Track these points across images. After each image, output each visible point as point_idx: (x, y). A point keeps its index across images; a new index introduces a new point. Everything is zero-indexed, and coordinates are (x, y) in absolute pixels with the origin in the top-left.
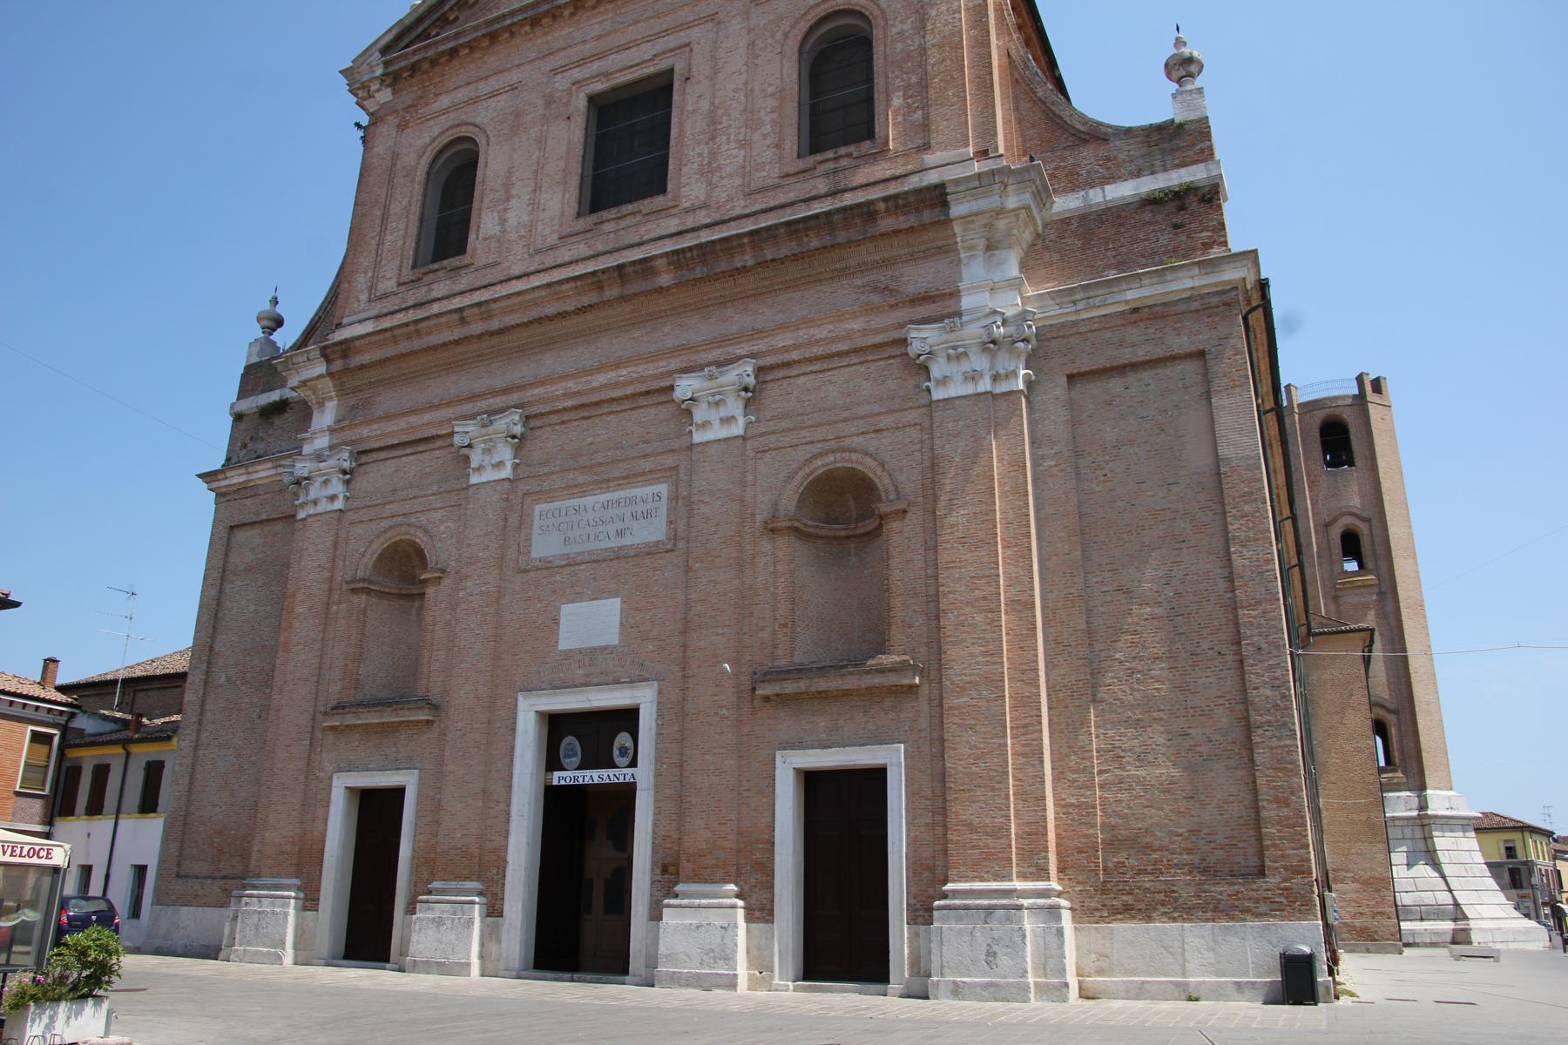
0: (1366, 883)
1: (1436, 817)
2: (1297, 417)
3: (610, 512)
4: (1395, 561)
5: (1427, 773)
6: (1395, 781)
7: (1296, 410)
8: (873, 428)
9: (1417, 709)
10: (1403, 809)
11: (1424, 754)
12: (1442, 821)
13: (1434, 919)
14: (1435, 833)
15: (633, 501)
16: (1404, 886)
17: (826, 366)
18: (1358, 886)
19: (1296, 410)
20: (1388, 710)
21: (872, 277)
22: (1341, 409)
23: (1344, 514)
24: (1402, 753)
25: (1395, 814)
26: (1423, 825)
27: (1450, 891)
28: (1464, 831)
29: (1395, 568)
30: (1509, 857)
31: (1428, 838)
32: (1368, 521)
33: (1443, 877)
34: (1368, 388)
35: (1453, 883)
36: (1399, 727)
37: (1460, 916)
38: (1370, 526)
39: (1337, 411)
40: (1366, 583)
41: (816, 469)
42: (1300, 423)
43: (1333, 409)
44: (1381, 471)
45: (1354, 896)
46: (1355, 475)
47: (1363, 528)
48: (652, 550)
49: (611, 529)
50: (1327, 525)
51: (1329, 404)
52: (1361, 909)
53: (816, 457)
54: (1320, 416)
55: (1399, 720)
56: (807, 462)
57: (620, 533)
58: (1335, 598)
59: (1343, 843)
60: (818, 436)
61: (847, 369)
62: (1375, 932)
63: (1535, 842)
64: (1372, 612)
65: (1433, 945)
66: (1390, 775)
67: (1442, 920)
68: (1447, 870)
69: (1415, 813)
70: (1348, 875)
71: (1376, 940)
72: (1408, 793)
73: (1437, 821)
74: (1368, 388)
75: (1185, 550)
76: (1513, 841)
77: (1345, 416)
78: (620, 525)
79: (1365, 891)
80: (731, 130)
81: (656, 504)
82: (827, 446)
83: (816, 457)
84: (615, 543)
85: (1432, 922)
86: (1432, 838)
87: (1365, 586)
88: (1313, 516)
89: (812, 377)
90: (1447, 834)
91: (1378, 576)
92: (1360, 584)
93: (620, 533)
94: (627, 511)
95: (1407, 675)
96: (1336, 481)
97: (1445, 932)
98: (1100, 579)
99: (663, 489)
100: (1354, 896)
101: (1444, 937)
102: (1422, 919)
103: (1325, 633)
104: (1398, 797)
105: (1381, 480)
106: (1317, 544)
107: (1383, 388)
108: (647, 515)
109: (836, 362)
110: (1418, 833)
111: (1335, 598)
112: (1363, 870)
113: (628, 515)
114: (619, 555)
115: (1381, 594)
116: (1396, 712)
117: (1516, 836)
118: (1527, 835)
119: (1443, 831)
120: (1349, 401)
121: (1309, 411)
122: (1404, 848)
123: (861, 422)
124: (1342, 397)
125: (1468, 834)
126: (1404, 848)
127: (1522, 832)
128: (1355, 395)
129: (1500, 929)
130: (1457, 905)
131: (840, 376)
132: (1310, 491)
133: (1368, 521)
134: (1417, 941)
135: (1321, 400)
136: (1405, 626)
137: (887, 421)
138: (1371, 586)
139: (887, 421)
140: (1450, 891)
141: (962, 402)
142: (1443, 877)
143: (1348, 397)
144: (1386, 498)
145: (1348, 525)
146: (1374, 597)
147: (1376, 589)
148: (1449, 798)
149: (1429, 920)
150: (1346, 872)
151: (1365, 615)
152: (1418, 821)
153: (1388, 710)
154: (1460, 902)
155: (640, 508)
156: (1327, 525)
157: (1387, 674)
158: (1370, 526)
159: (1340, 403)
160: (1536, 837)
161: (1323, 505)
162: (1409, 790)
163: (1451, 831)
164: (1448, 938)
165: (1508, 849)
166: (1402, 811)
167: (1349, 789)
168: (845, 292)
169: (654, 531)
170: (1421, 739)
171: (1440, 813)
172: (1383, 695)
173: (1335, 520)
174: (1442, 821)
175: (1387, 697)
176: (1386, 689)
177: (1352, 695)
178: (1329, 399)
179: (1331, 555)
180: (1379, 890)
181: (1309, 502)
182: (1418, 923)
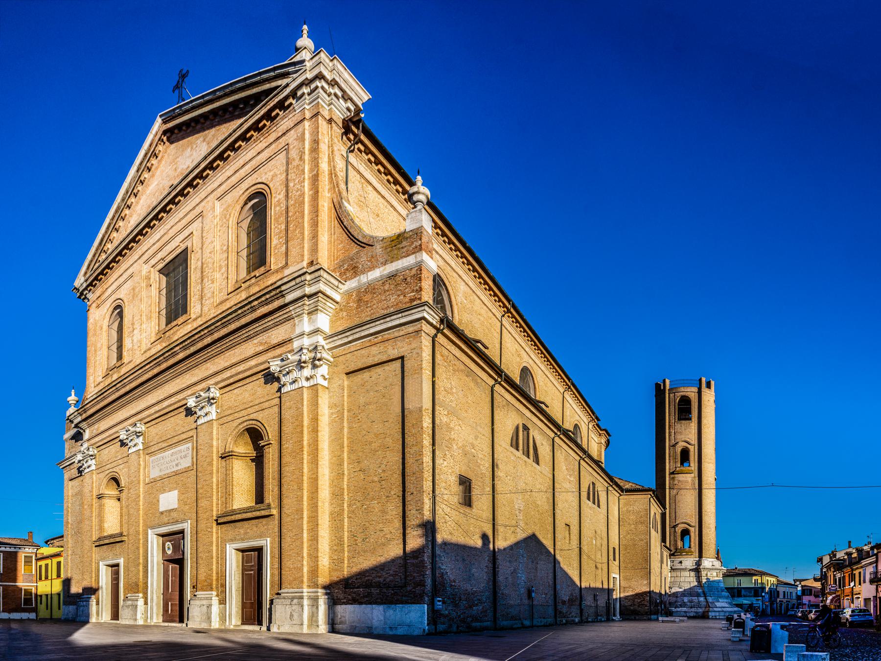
3: (174, 457)
8: (261, 409)
15: (180, 451)
17: (244, 383)
21: (261, 338)
41: (240, 430)
48: (187, 470)
49: (174, 464)
53: (240, 424)
56: (237, 426)
57: (177, 465)
60: (241, 415)
61: (253, 383)
75: (388, 452)
78: (177, 462)
80: (209, 274)
81: (188, 452)
82: (245, 419)
83: (240, 424)
84: (175, 469)
89: (239, 389)
93: (177, 465)
94: (179, 456)
98: (353, 466)
99: (190, 445)
108: (185, 456)
109: (247, 380)
113: (179, 458)
114: (176, 474)
123: (256, 407)
131: (249, 387)
137: (266, 405)
139: (266, 405)
141: (293, 392)
155: (183, 454)
168: (250, 347)
169: (186, 463)
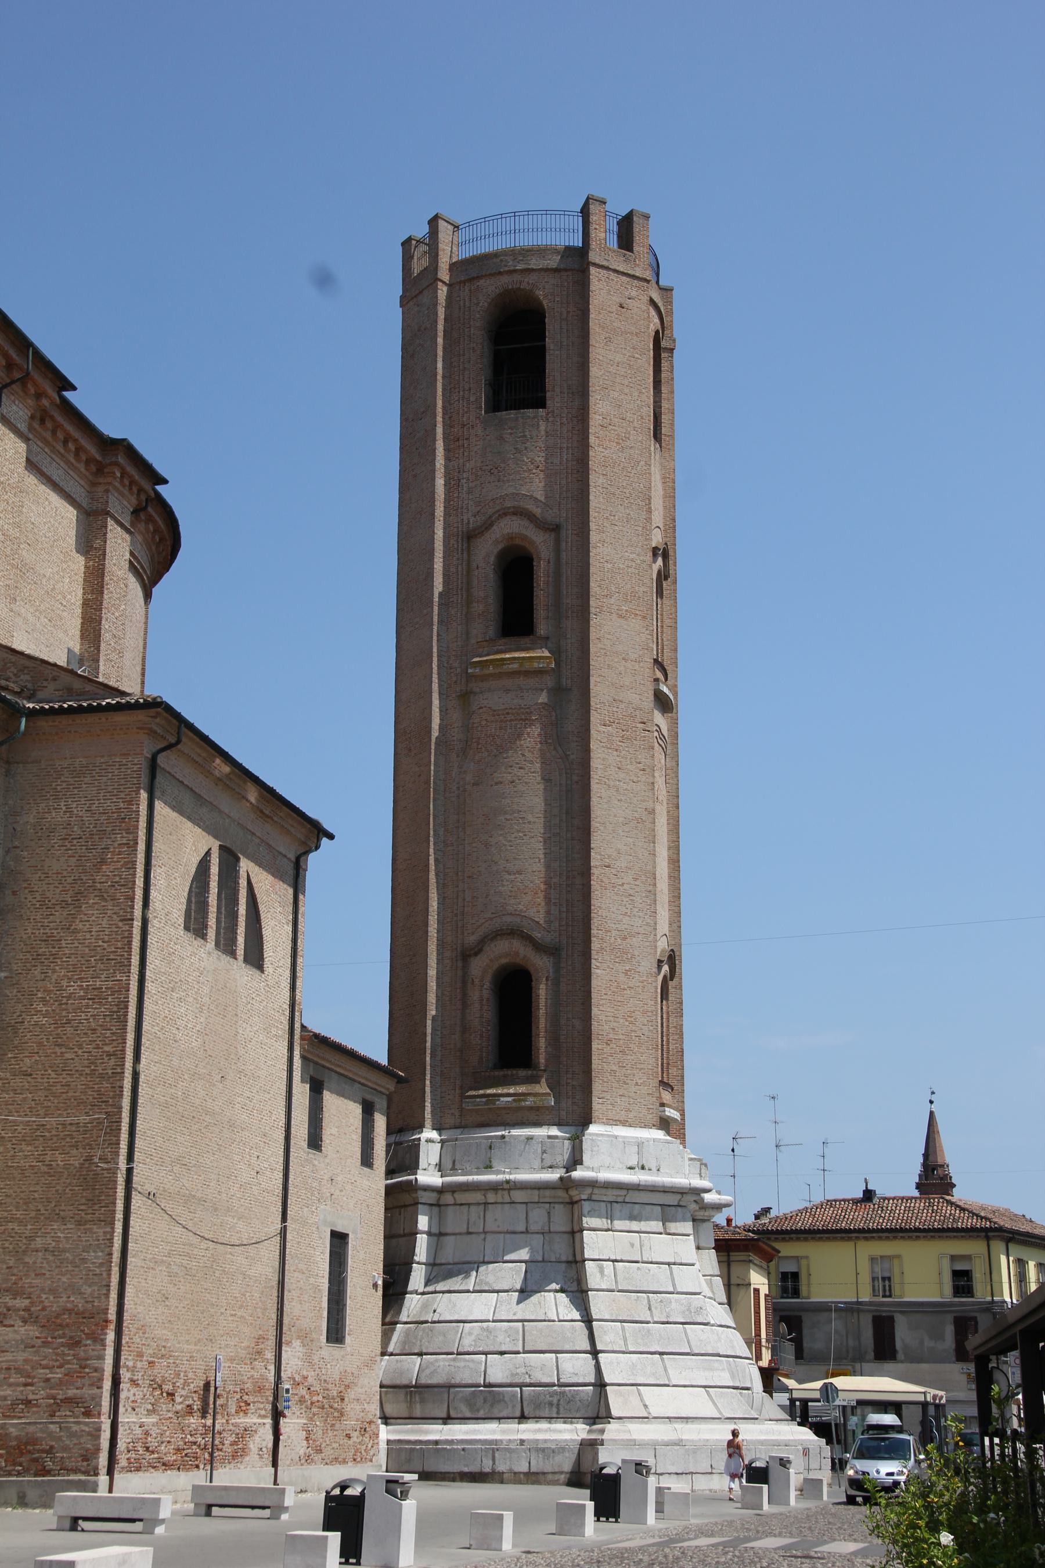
0: (52, 1324)
1: (593, 1184)
2: (442, 292)
4: (594, 621)
5: (597, 1087)
6: (529, 1102)
7: (444, 274)
9: (595, 945)
10: (537, 1164)
11: (595, 1046)
12: (611, 1194)
13: (550, 1419)
14: (588, 1221)
16: (500, 1338)
18: (32, 1331)
19: (444, 274)
20: (538, 947)
22: (532, 278)
23: (504, 513)
24: (554, 1040)
25: (512, 1177)
26: (572, 1203)
27: (595, 1353)
28: (665, 1220)
29: (593, 635)
30: (958, 1291)
31: (575, 1233)
32: (555, 529)
33: (588, 1320)
34: (605, 235)
35: (607, 1335)
36: (556, 983)
37: (603, 1413)
38: (558, 542)
39: (526, 282)
40: (527, 666)
42: (447, 307)
43: (517, 277)
44: (595, 420)
45: (21, 1356)
46: (542, 428)
47: (541, 544)
50: (470, 536)
51: (511, 265)
52: (29, 1393)
54: (490, 288)
55: (557, 968)
58: (465, 697)
59: (20, 1222)
62: (50, 1450)
63: (1021, 1263)
64: (536, 730)
65: (532, 1477)
66: (521, 1089)
67: (566, 1419)
68: (599, 1306)
69: (554, 1176)
70: (21, 1303)
71: (47, 1472)
72: (554, 1131)
73: (598, 1194)
74: (605, 235)
76: (968, 1258)
77: (540, 293)
79: (46, 1344)
85: (544, 1425)
86: (581, 1231)
87: (527, 673)
88: (447, 514)
90: (618, 1224)
91: (557, 653)
92: (515, 666)
95: (586, 872)
96: (501, 438)
97: (560, 1449)
100: (21, 1356)
101: (558, 1458)
102: (523, 1418)
103: (61, 711)
104: (530, 1138)
105: (592, 439)
106: (446, 576)
107: (637, 238)
110: (560, 1222)
111: (465, 697)
112: (53, 1291)
115: (558, 692)
116: (553, 951)
117: (974, 1248)
118: (998, 1246)
119: (611, 1218)
120: (554, 261)
121: (471, 280)
122: (524, 1254)
124: (541, 251)
125: (673, 1227)
126: (524, 1254)
127: (988, 1239)
128: (568, 249)
129: (679, 1443)
130: (601, 1385)
132: (448, 459)
133: (555, 529)
134: (501, 1467)
135: (495, 255)
136: (595, 763)
138: (540, 672)
140: (595, 1353)
142: (588, 1320)
143: (554, 250)
144: (597, 481)
145: (511, 537)
146: (543, 698)
147: (549, 681)
148: (640, 1145)
149: (538, 1418)
150: (16, 1295)
151: (519, 736)
152: (561, 1193)
153: (538, 947)
154: (607, 1380)
156: (470, 536)
157: (548, 867)
158: (558, 542)
159: (535, 263)
160: (1016, 1251)
161: (470, 491)
162: (559, 1124)
163: (632, 1218)
164: (567, 1463)
165: (957, 1274)
166: (533, 1170)
167: (58, 1089)
170: (595, 1011)
171: (604, 1175)
172: (531, 913)
173: (488, 526)
174: (611, 1194)
175: (541, 918)
176: (540, 899)
177: (103, 861)
178: (515, 253)
179: (469, 603)
180: (78, 1343)
181: (440, 482)
182: (514, 1426)
